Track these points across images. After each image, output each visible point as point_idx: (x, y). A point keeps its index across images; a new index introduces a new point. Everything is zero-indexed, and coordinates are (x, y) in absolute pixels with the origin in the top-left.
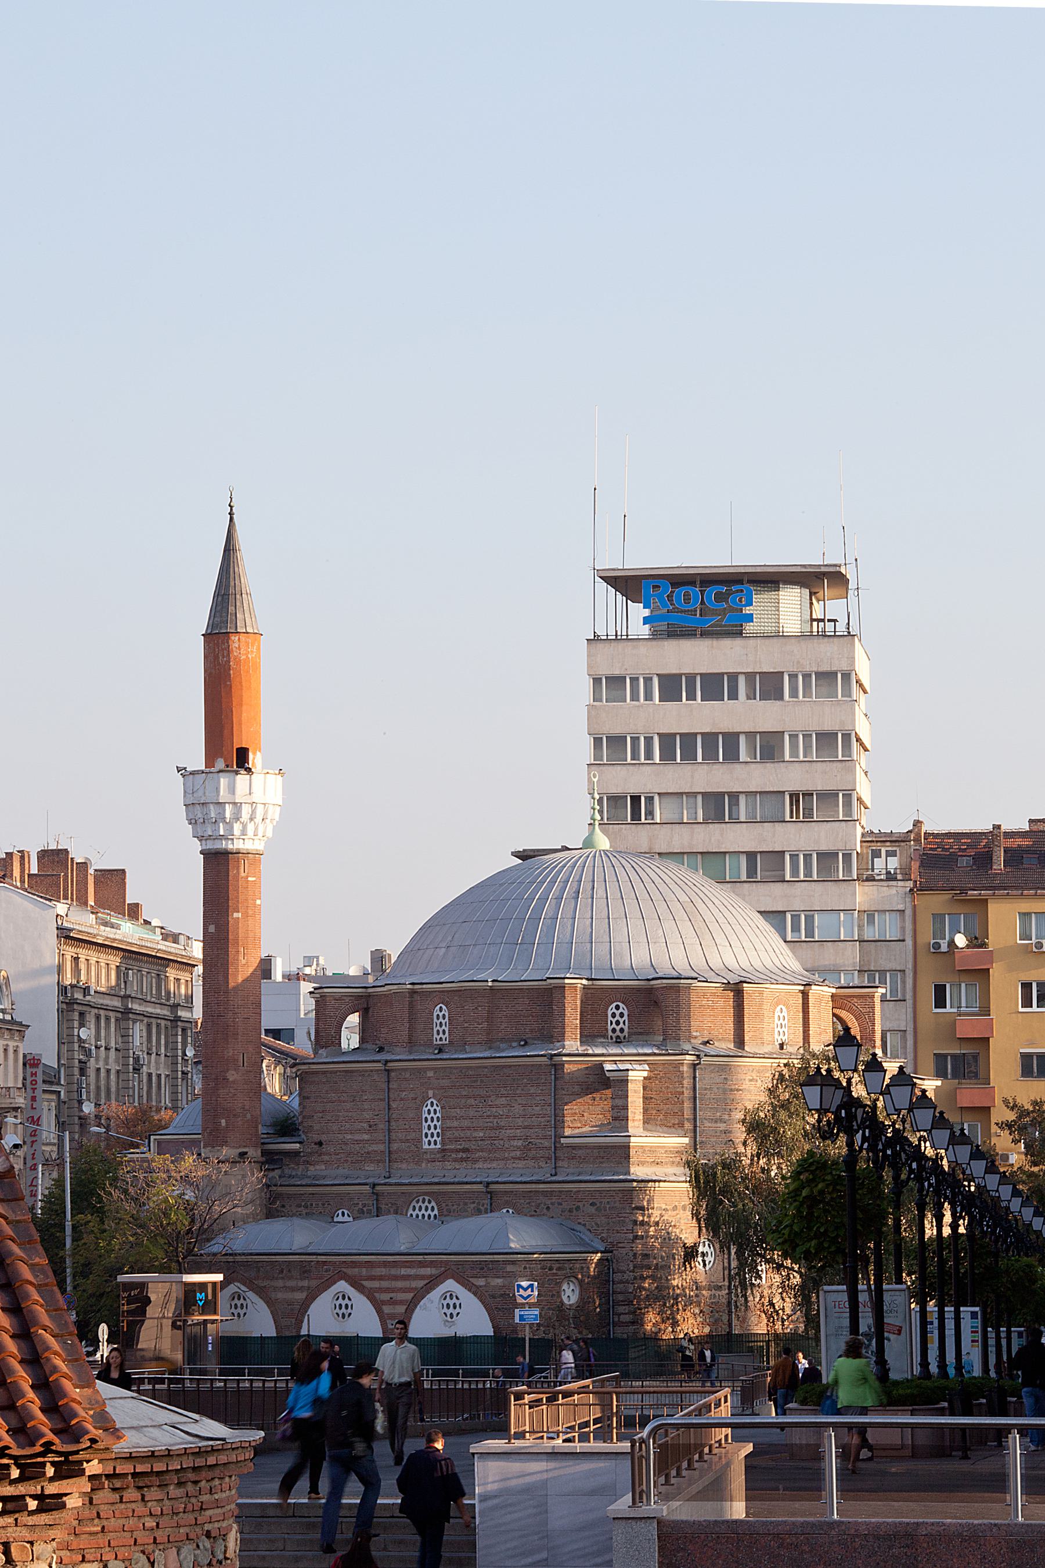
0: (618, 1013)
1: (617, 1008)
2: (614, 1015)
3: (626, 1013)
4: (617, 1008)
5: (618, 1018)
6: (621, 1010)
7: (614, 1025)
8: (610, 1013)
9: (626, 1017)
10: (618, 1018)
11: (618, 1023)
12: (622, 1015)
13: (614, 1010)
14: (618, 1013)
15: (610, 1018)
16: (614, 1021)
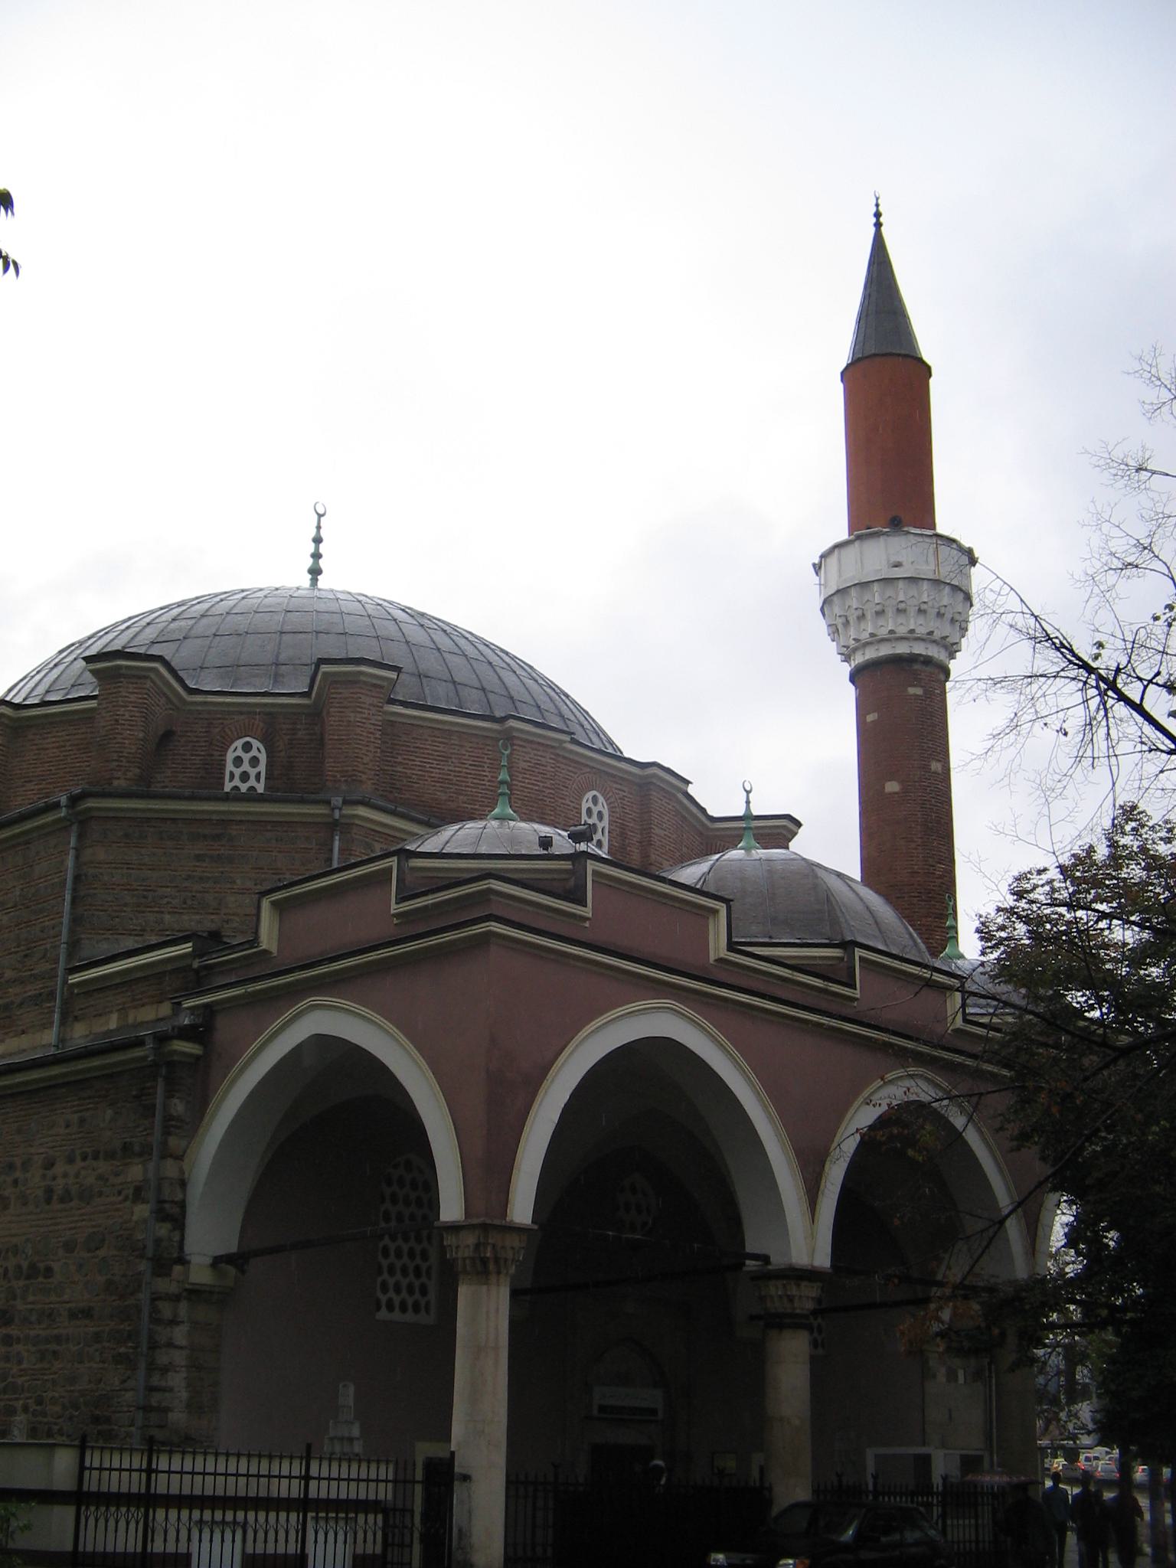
0: (246, 757)
1: (247, 747)
2: (238, 761)
3: (263, 758)
4: (247, 747)
5: (246, 767)
6: (254, 753)
7: (237, 782)
8: (230, 756)
9: (262, 767)
10: (246, 767)
11: (245, 777)
12: (254, 761)
13: (240, 753)
14: (246, 757)
15: (230, 767)
16: (237, 772)
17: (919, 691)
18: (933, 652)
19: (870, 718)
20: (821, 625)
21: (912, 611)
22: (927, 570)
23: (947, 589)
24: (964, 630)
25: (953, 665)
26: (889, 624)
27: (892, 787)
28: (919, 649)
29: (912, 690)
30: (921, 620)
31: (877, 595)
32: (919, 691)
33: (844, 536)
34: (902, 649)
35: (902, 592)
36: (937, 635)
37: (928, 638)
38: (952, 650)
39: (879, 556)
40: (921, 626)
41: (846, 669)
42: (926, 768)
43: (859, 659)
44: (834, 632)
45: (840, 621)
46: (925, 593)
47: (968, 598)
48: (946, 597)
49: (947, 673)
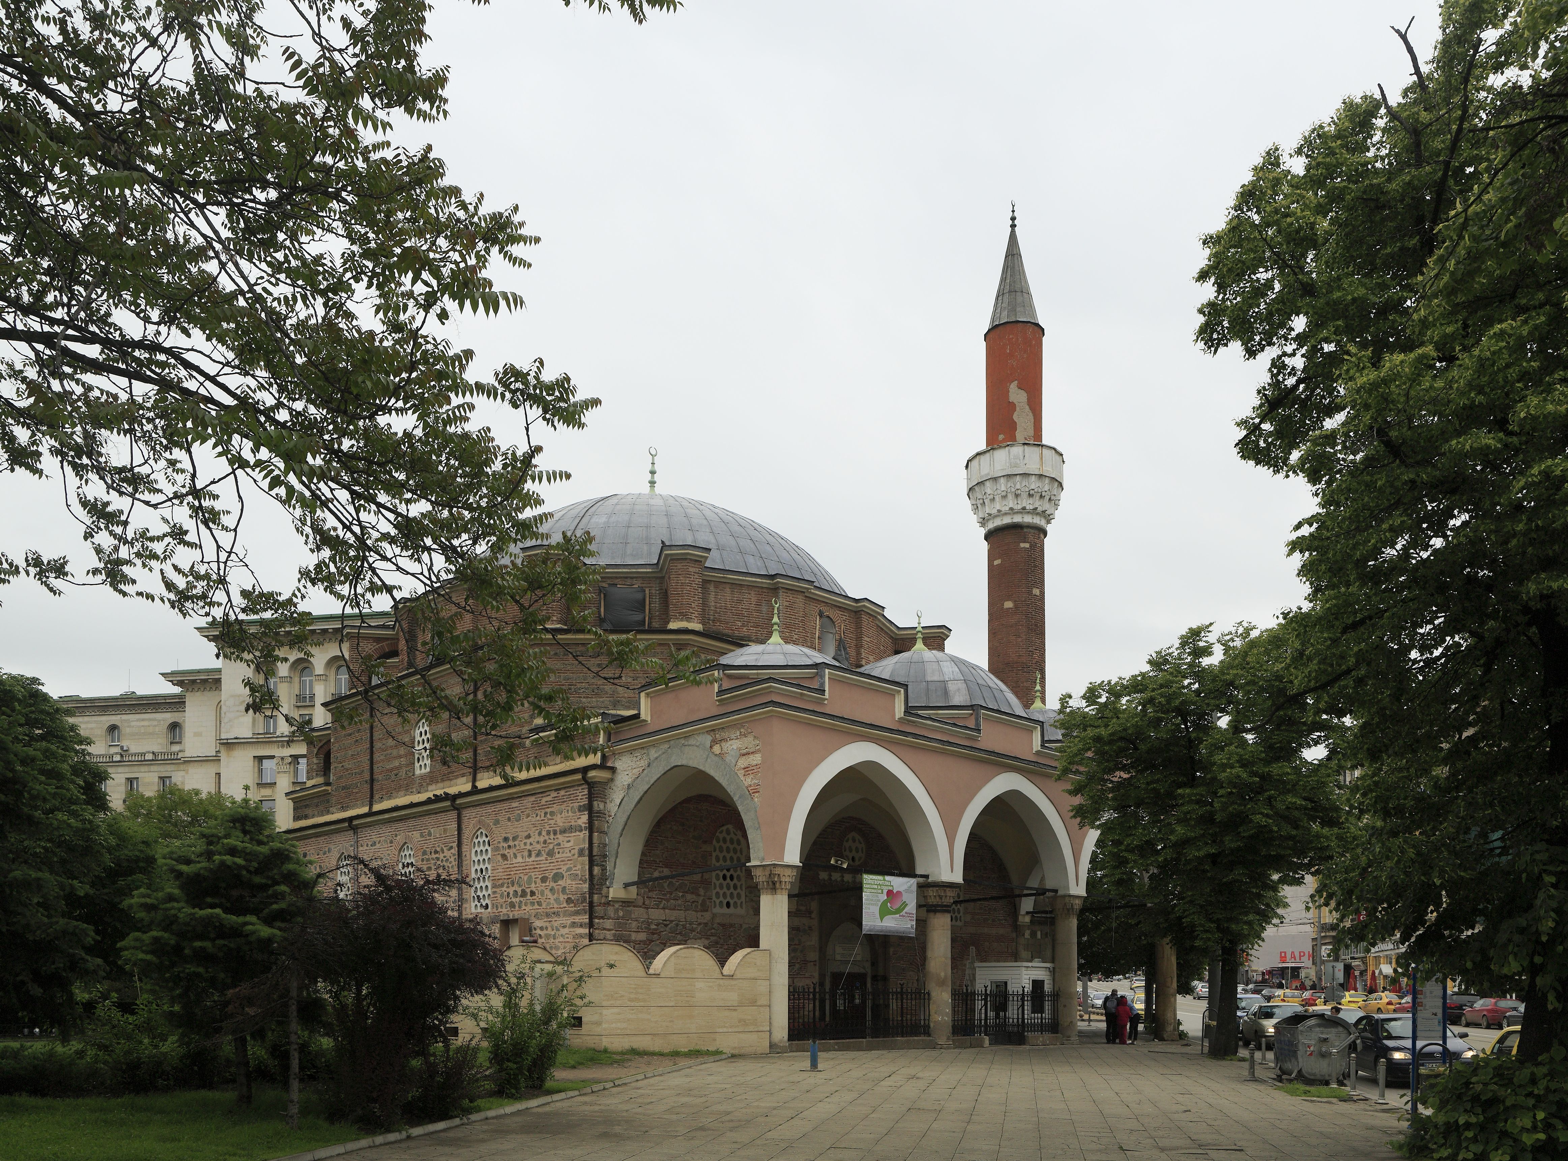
17: (1027, 545)
18: (1038, 521)
19: (997, 562)
20: (967, 503)
21: (1025, 495)
22: (1033, 467)
23: (1047, 480)
24: (1057, 505)
25: (1049, 528)
26: (1011, 503)
27: (1009, 604)
28: (1028, 519)
29: (1022, 545)
30: (1031, 501)
31: (1003, 485)
32: (1027, 545)
33: (983, 446)
34: (1017, 519)
35: (1019, 484)
36: (1040, 509)
37: (1034, 512)
38: (1049, 519)
39: (1003, 460)
40: (1029, 504)
41: (982, 532)
42: (1030, 593)
43: (991, 525)
44: (976, 508)
45: (979, 502)
46: (1034, 484)
47: (1060, 485)
48: (1046, 486)
49: (1045, 533)
